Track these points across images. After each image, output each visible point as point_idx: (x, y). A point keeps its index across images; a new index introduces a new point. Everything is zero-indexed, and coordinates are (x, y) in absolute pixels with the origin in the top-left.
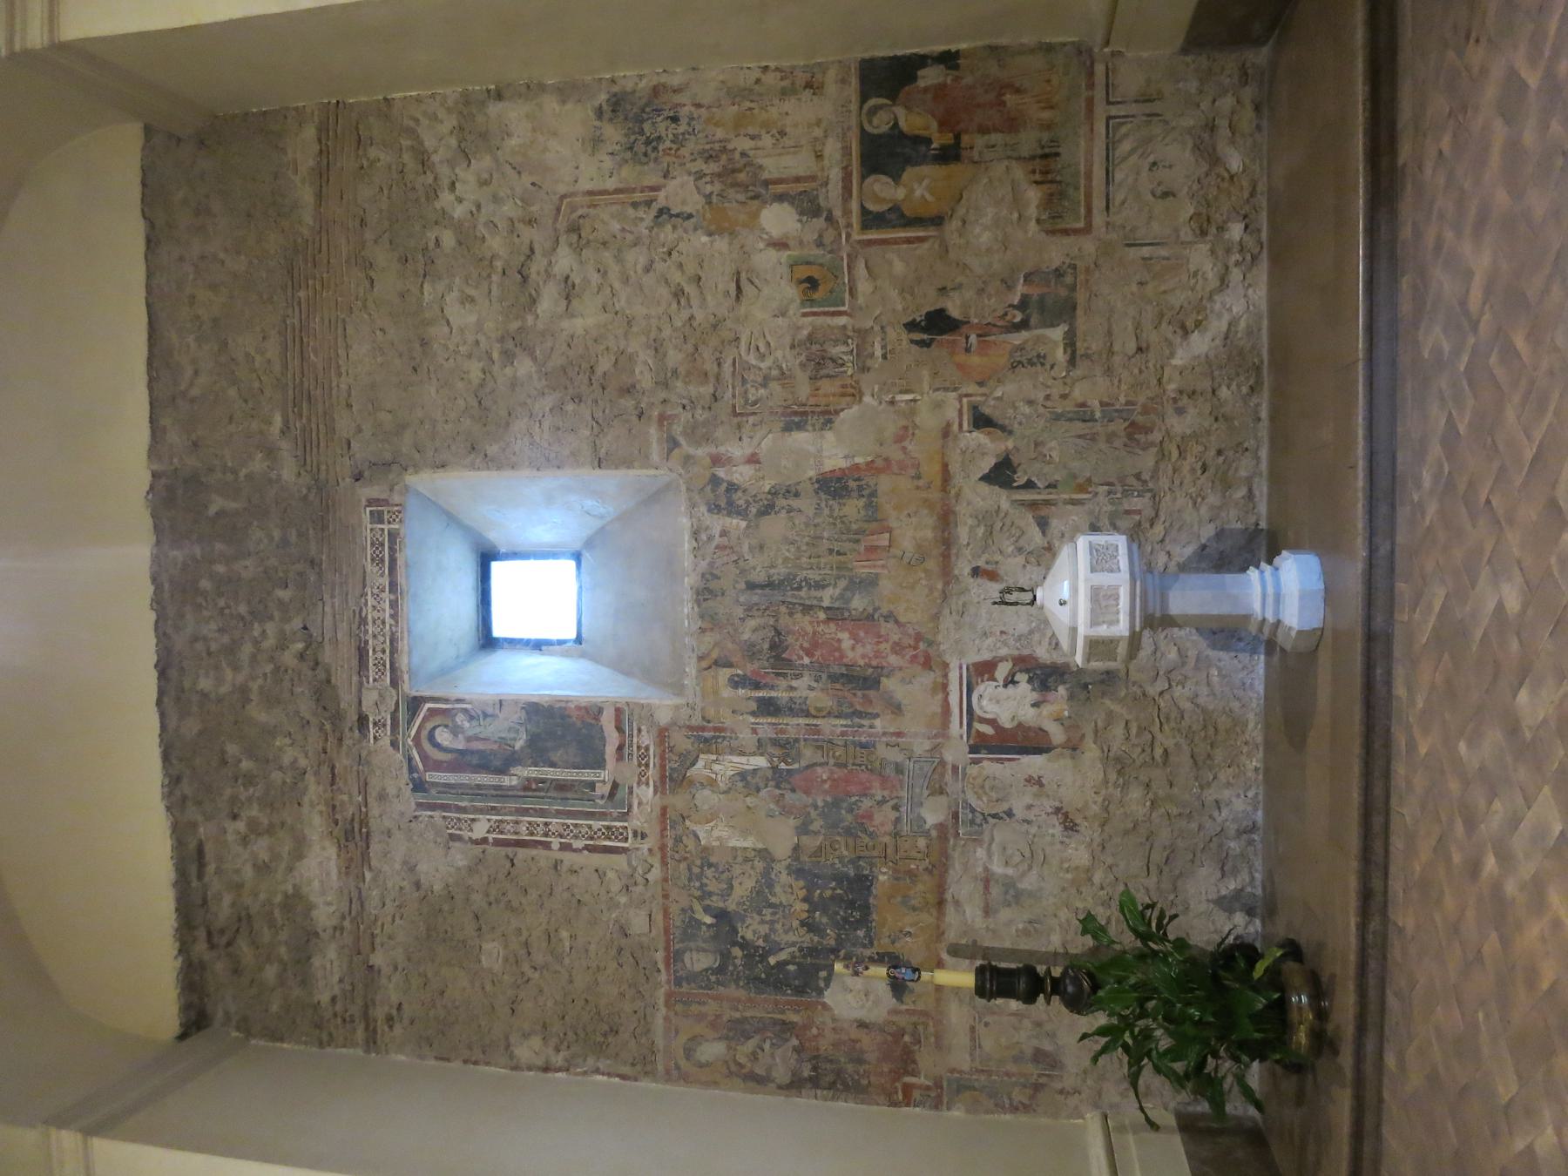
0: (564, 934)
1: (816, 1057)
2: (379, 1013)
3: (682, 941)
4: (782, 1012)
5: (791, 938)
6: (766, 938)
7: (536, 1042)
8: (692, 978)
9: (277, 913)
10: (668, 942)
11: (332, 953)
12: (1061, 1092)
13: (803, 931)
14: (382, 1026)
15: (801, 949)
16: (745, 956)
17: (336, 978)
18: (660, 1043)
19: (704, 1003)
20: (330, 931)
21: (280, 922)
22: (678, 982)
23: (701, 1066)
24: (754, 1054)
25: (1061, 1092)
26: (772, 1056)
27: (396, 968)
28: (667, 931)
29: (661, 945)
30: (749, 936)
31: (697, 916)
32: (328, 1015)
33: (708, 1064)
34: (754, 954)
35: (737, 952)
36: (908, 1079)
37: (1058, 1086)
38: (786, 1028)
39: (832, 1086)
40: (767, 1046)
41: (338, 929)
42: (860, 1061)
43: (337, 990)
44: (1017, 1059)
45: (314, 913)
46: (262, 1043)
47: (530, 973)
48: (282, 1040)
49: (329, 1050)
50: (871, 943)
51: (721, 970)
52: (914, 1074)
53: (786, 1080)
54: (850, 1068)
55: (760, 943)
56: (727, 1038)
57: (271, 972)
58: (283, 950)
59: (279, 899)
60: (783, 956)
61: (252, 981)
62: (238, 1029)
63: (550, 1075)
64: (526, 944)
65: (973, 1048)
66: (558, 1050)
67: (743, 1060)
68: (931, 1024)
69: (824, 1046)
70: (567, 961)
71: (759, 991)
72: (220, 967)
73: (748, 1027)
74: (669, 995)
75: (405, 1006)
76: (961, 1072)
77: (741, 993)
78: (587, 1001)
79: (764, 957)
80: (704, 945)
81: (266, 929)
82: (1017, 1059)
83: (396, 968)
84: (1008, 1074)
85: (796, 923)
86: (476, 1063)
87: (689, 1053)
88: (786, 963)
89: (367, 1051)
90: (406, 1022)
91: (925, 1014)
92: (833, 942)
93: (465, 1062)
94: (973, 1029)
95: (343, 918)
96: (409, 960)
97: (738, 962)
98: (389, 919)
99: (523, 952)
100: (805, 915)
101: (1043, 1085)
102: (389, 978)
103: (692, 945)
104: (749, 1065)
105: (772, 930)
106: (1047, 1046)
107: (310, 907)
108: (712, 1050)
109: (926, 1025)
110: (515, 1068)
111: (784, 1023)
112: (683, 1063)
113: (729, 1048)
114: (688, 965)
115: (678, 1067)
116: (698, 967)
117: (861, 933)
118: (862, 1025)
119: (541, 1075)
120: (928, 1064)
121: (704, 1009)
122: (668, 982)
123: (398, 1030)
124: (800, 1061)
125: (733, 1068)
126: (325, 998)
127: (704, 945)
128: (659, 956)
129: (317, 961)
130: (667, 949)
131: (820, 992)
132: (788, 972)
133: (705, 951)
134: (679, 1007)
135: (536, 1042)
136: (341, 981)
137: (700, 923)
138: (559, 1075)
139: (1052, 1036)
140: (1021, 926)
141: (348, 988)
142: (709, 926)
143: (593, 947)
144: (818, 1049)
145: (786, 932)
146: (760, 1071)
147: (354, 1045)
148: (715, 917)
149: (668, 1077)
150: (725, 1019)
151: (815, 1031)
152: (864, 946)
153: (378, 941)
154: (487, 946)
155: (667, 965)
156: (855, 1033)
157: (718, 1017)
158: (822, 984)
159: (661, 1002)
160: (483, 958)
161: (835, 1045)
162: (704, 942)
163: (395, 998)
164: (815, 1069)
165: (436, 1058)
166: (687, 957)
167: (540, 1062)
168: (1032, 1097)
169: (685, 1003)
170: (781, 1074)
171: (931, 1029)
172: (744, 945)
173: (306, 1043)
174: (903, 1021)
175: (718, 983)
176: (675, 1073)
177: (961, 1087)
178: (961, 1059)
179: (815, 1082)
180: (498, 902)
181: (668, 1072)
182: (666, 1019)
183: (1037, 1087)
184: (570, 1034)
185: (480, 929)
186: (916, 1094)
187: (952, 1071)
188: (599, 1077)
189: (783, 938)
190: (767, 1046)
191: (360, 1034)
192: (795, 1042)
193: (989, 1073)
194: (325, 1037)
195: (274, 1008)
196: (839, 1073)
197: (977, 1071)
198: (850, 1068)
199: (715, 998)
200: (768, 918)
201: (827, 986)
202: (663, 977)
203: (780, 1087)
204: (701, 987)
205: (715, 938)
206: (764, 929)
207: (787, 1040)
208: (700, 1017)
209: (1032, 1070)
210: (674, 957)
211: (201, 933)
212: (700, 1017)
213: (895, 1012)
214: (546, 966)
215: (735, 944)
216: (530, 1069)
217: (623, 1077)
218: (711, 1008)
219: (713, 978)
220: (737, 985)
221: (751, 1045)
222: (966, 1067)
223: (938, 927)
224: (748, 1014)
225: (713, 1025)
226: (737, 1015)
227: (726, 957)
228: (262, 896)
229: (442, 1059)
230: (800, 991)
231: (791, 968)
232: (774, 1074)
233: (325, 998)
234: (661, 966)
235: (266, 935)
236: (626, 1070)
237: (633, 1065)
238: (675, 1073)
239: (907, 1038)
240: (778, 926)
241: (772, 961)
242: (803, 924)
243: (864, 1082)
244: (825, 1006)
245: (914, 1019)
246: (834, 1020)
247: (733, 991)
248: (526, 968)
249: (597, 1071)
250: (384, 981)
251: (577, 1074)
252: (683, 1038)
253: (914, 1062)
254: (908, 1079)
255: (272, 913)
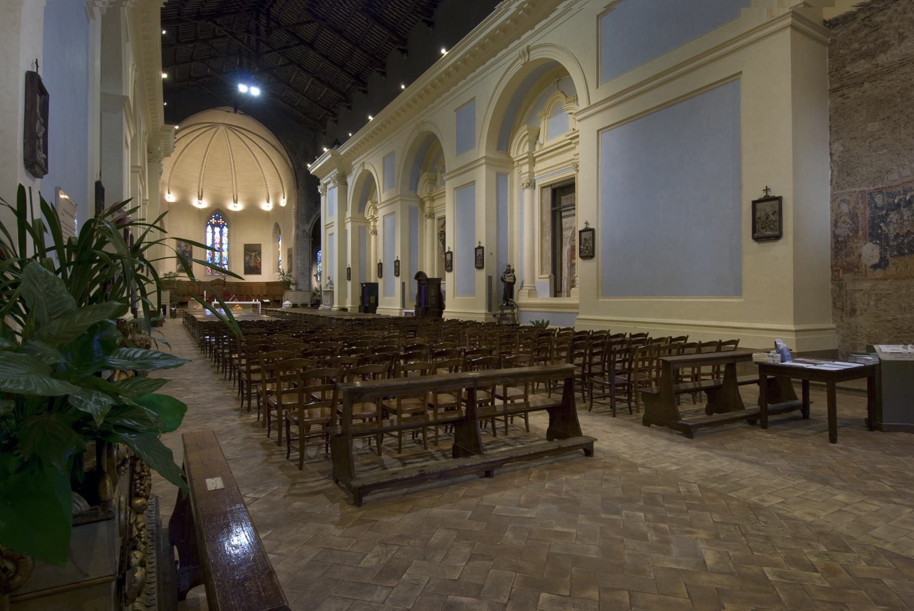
0: (885, 151)
1: (846, 242)
2: (845, 91)
3: (887, 193)
4: (862, 230)
5: (892, 230)
6: (891, 222)
7: (841, 149)
8: (872, 198)
9: (881, 40)
10: (886, 188)
11: (867, 66)
12: (842, 316)
13: (895, 234)
14: (840, 93)
15: (887, 234)
16: (883, 215)
17: (857, 71)
18: (848, 190)
19: (862, 204)
20: (875, 63)
21: (876, 43)
22: (870, 194)
23: (839, 205)
24: (845, 222)
25: (842, 316)
26: (844, 228)
27: (863, 93)
28: (890, 187)
29: (884, 186)
30: (891, 216)
31: (897, 197)
32: (842, 72)
33: (839, 208)
34: (883, 219)
35: (884, 212)
36: (841, 271)
37: (844, 315)
38: (857, 232)
39: (836, 247)
40: (848, 226)
41: (877, 66)
42: (846, 255)
43: (851, 72)
44: (852, 304)
45: (882, 55)
46: (827, 51)
47: (868, 141)
48: (830, 58)
49: (828, 76)
50: (892, 257)
51: (876, 207)
52: (843, 273)
53: (837, 233)
54: (844, 252)
55: (889, 220)
56: (850, 213)
57: (856, 45)
58: (865, 47)
59: (887, 39)
60: (884, 228)
61: (851, 40)
62: (831, 40)
63: (829, 156)
64: (880, 138)
65: (855, 290)
66: (839, 157)
67: (842, 219)
68: (863, 277)
69: (851, 244)
70: (874, 154)
71: (869, 222)
72: (855, 25)
73: (855, 219)
74: (864, 191)
75: (849, 100)
76: (845, 287)
77: (868, 215)
78: (859, 163)
79: (883, 221)
80: (885, 201)
81: (872, 38)
82: (852, 304)
83: (863, 93)
84: (846, 301)
85: (897, 231)
86: (830, 130)
87: (843, 201)
88: (881, 229)
89: (830, 90)
90: (843, 101)
91: (866, 275)
92: (891, 244)
93: (830, 126)
94: (862, 290)
95: (882, 66)
96: (867, 97)
97: (880, 213)
98: (884, 85)
99: (876, 137)
100: (901, 234)
101: (843, 311)
102: (859, 91)
103: (885, 197)
104: (841, 221)
105: (894, 223)
106: (858, 313)
107: (885, 52)
108: (845, 208)
109: (862, 275)
110: (830, 144)
111: (858, 231)
112: (839, 199)
113: (846, 213)
114: (877, 196)
115: (837, 198)
116: (877, 200)
117: (896, 253)
118: (860, 256)
119: (828, 153)
120: (848, 276)
121: (861, 204)
122: (870, 190)
123: (839, 99)
124: (844, 237)
125: (839, 216)
126: (848, 69)
127: (885, 201)
128: (880, 186)
129: (862, 62)
130: (883, 188)
131: (871, 241)
132: (878, 230)
133: (884, 201)
134: (860, 195)
135: (841, 149)
136: (856, 73)
137: (894, 198)
138: (830, 159)
139: (862, 314)
140: (903, 305)
141: (853, 76)
142: (894, 201)
143: (881, 162)
144: (849, 242)
145: (893, 228)
146: (839, 224)
147: (831, 84)
148: (898, 203)
149: (832, 195)
150: (857, 211)
151: (856, 241)
152: (891, 254)
153: (874, 83)
154: (877, 123)
155: (875, 189)
156: (856, 254)
157: (858, 209)
158: (874, 242)
159: (861, 189)
160: (872, 123)
161: (851, 248)
162: (887, 201)
163: (852, 95)
164: (842, 242)
165: (830, 116)
166: (880, 195)
167: (833, 152)
168: (839, 308)
169: (862, 197)
170: (838, 231)
171: (860, 277)
172: (887, 215)
173: (829, 67)
174: (863, 268)
175: (871, 207)
176: (835, 197)
177: (840, 287)
178: (850, 287)
179: (837, 242)
180: (896, 124)
181: (835, 195)
182: (855, 192)
183: (843, 310)
184: (845, 160)
185: (883, 119)
186: (836, 274)
187: (846, 284)
188: (830, 172)
189: (891, 228)
190: (848, 226)
191: (836, 85)
192: (851, 235)
193: (846, 295)
194: (832, 74)
195: (841, 51)
196: (841, 249)
197: (846, 292)
198: (844, 252)
199: (865, 208)
200: (899, 221)
201: (874, 243)
202: (872, 188)
203: (834, 232)
204: (869, 202)
205: (889, 204)
206: (894, 220)
207: (851, 232)
208: (857, 203)
209: (849, 308)
210: (880, 191)
211: (868, 14)
212: (857, 203)
213: (866, 266)
214: (870, 146)
215: (887, 211)
216: (830, 149)
217: (831, 181)
218: (861, 206)
219: (873, 205)
220: (870, 214)
221: (848, 220)
222: (847, 288)
223: (901, 278)
224: (860, 218)
225: (855, 207)
226: (859, 215)
227: (882, 209)
228: (887, 32)
229: (830, 118)
230: (871, 234)
231: (880, 231)
232: (839, 229)
233: (848, 69)
234: (875, 187)
235: (870, 39)
236: (834, 182)
237: (836, 183)
238: (835, 197)
239: (856, 270)
240: (896, 225)
241: (882, 224)
242: (898, 233)
243: (839, 257)
244: (865, 244)
245: (864, 272)
246: (861, 247)
247: (868, 213)
248: (870, 140)
249: (832, 172)
250: (858, 89)
251: (830, 165)
252: (847, 198)
253: (848, 273)
254: (841, 271)
255: (881, 38)
